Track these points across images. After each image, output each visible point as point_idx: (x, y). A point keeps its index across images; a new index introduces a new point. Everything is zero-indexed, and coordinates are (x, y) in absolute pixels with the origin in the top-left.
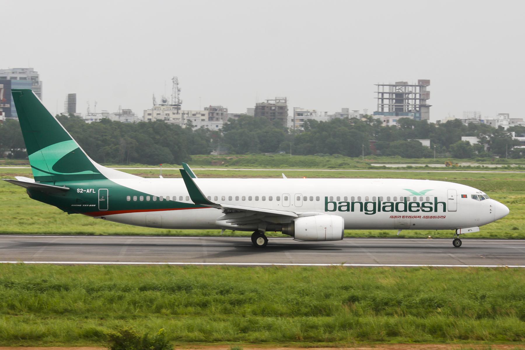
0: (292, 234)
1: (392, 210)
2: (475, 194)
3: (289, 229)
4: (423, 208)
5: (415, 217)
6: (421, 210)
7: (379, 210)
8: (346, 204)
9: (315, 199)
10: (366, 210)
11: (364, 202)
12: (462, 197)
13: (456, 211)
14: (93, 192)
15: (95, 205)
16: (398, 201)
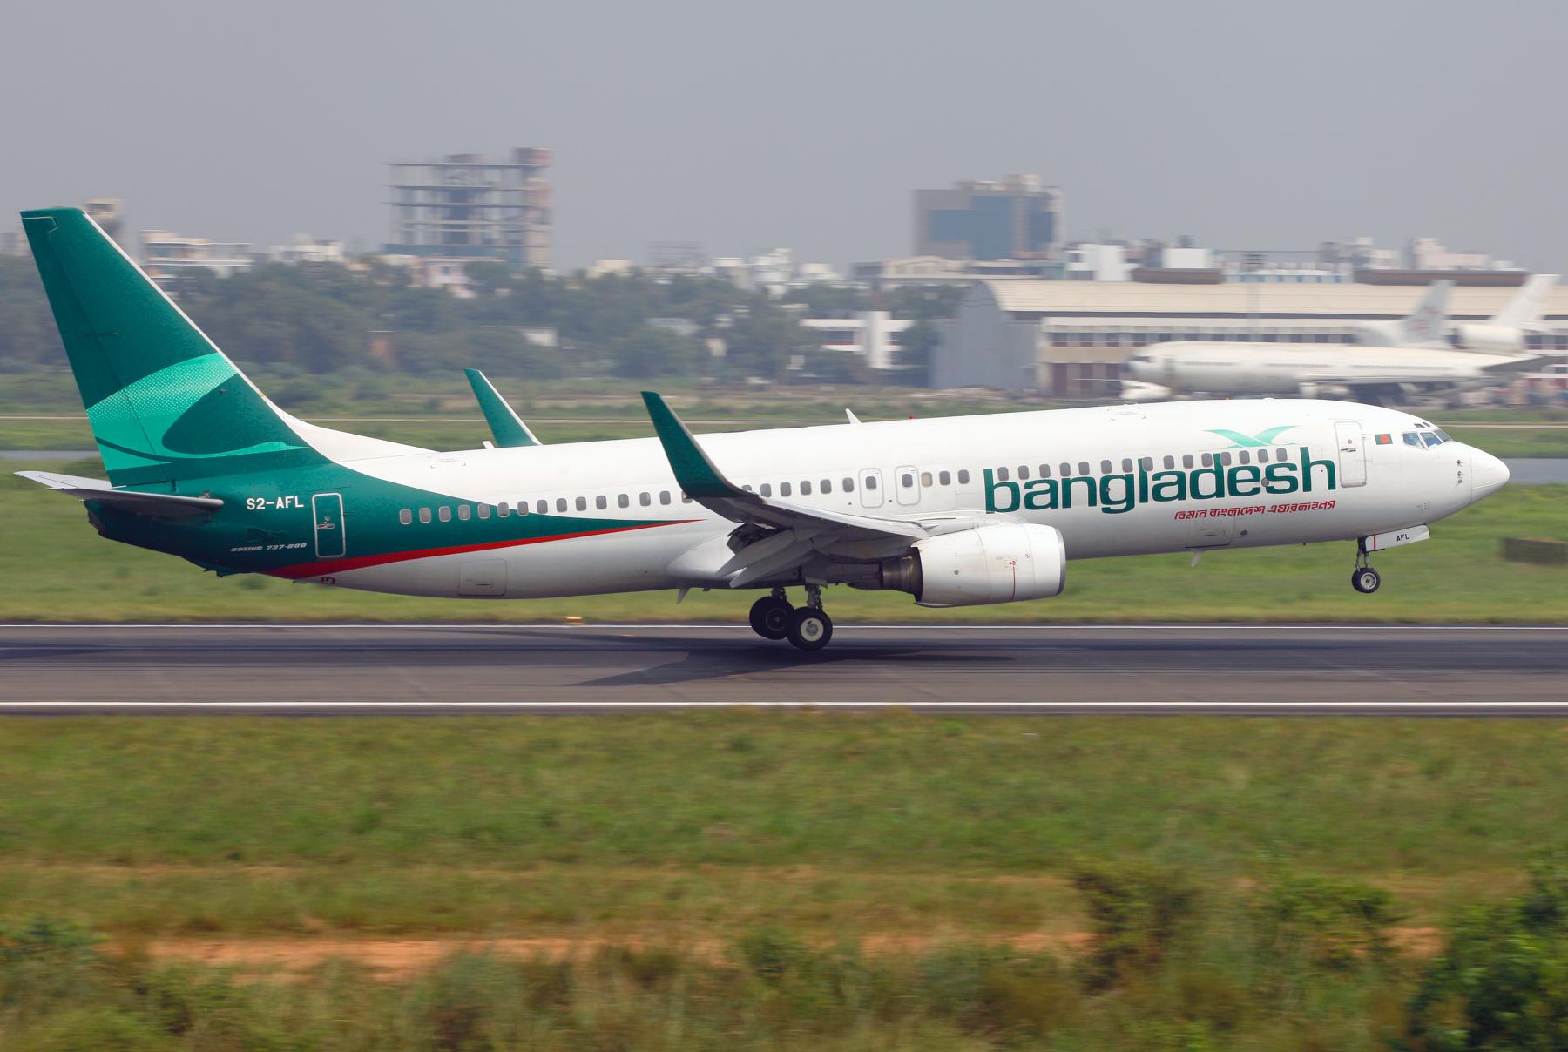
0: (915, 587)
1: (1181, 496)
2: (1412, 429)
3: (907, 572)
4: (1271, 484)
5: (1249, 510)
6: (1263, 489)
7: (1144, 499)
8: (1046, 487)
9: (954, 478)
10: (1106, 500)
11: (1097, 474)
12: (1379, 443)
13: (1364, 484)
14: (297, 506)
15: (304, 545)
16: (1198, 465)
